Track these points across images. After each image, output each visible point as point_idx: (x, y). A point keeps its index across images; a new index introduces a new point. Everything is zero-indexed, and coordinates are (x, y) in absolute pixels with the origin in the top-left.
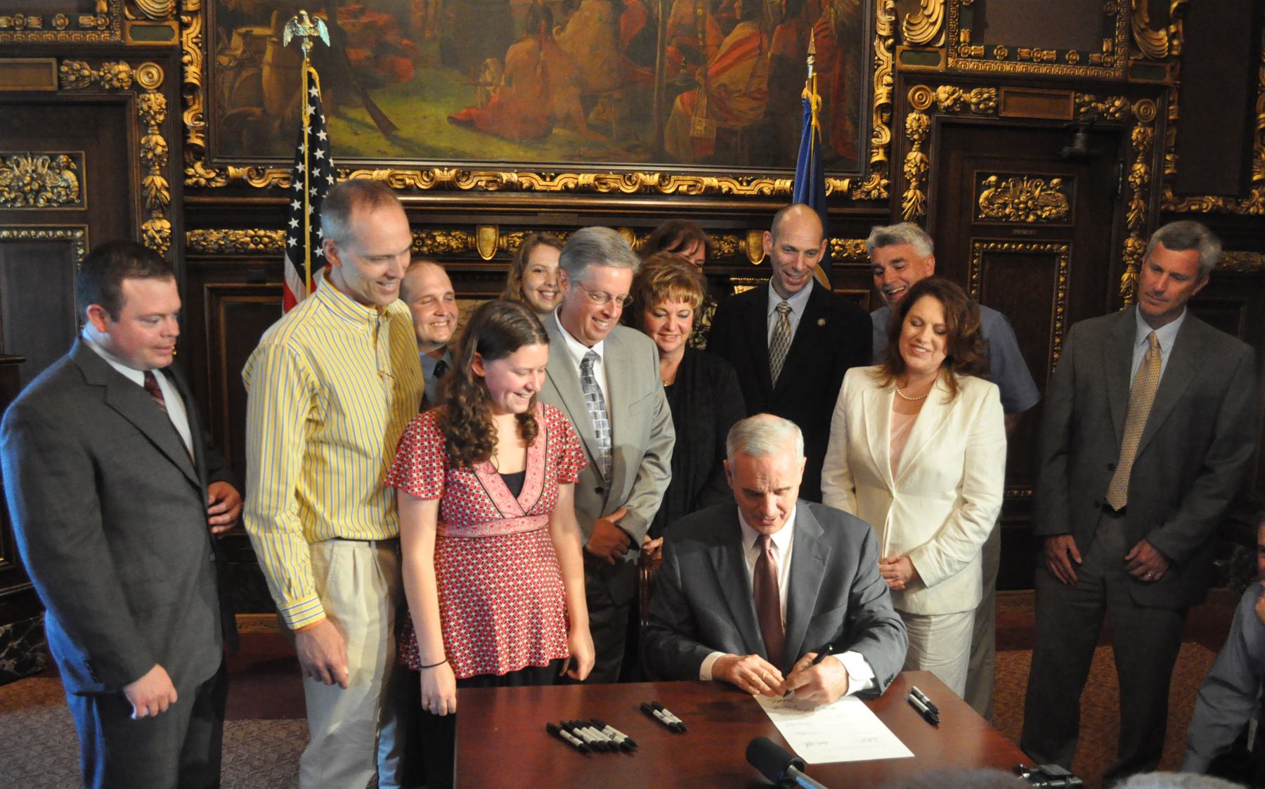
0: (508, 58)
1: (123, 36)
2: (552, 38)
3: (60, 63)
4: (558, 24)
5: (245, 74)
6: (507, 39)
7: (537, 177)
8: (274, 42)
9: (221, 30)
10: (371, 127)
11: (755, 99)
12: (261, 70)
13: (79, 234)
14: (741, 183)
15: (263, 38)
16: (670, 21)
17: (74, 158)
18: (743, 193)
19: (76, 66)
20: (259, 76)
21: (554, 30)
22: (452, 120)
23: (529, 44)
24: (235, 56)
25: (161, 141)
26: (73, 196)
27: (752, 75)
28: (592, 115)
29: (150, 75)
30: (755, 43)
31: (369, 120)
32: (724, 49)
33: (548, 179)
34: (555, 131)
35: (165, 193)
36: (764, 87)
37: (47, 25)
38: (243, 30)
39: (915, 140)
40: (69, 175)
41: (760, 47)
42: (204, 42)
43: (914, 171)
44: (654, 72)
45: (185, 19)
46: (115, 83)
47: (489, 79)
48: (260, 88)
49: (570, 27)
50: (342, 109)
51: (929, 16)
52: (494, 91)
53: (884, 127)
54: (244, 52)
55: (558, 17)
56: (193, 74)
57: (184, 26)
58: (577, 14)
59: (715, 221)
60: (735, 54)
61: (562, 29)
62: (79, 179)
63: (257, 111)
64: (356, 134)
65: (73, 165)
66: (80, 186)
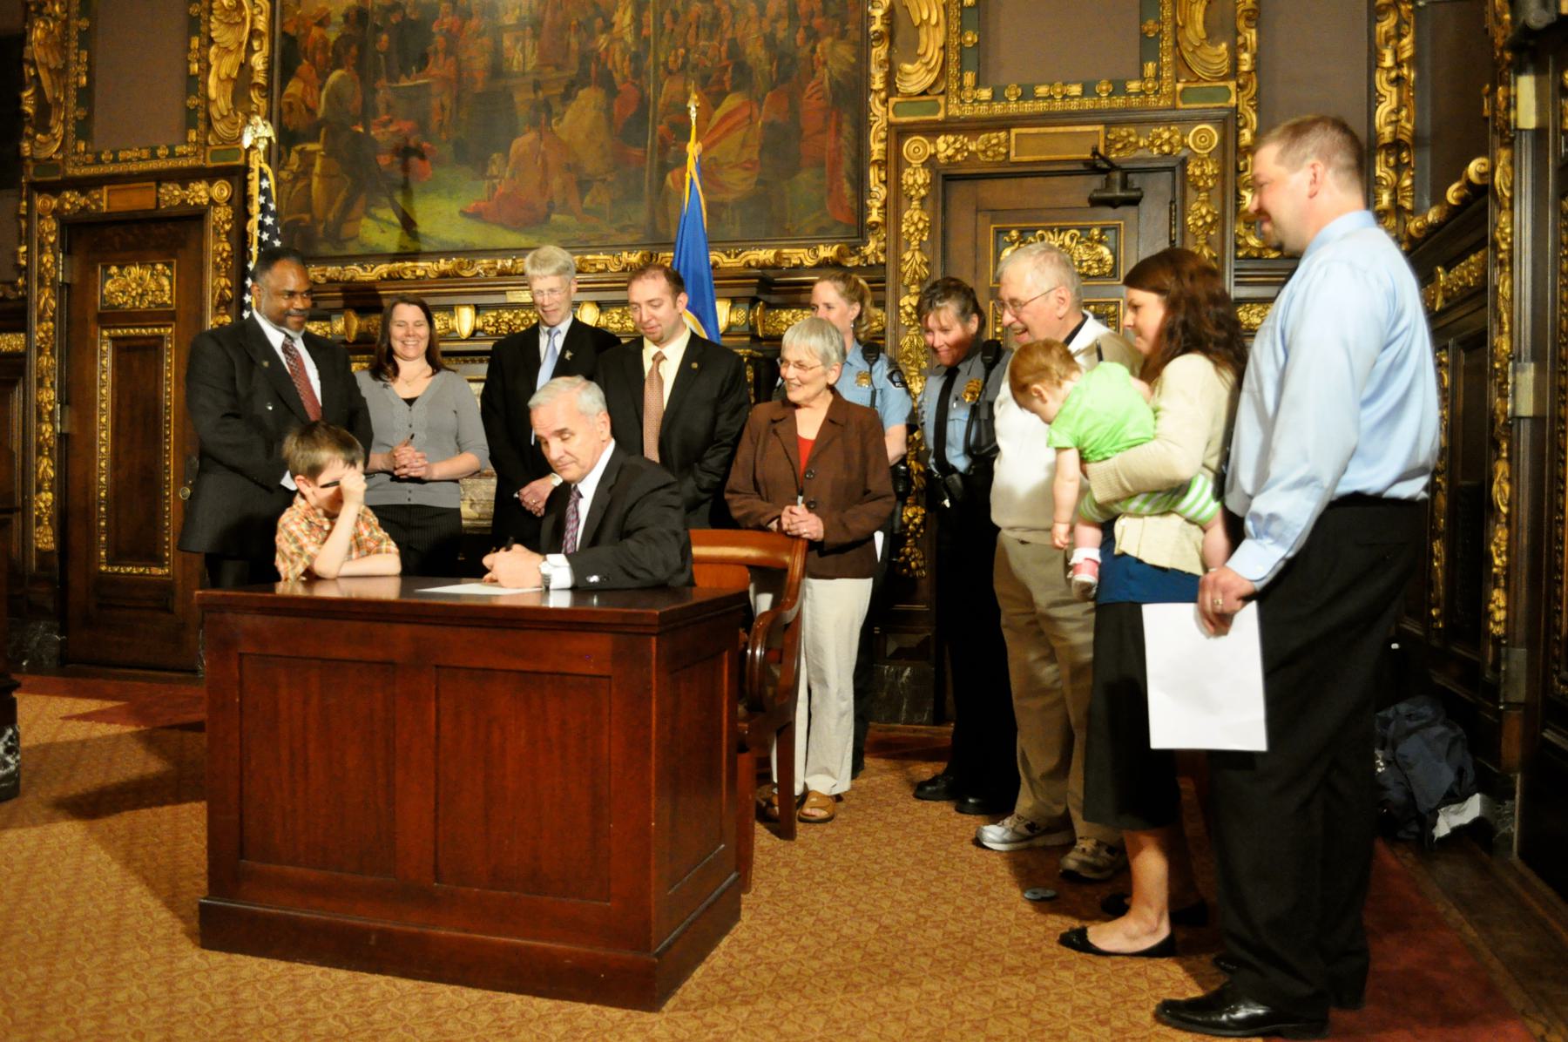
0: (512, 151)
2: (552, 131)
3: (159, 185)
4: (557, 114)
5: (300, 185)
6: (514, 134)
9: (283, 149)
10: (393, 224)
11: (747, 169)
12: (311, 180)
13: (170, 330)
14: (729, 256)
15: (314, 153)
16: (661, 100)
17: (169, 265)
19: (170, 188)
20: (309, 186)
22: (463, 213)
23: (530, 136)
24: (292, 172)
25: (228, 247)
26: (166, 298)
27: (744, 145)
28: (588, 199)
29: (221, 190)
30: (747, 112)
32: (714, 121)
34: (554, 217)
35: (228, 292)
36: (755, 156)
37: (154, 156)
38: (298, 147)
40: (165, 282)
41: (750, 117)
43: (912, 230)
44: (646, 152)
46: (198, 200)
47: (495, 173)
48: (310, 197)
49: (567, 117)
50: (373, 210)
51: (928, 63)
55: (557, 108)
58: (574, 104)
60: (725, 127)
61: (561, 120)
62: (171, 285)
63: (307, 217)
64: (383, 232)
65: (168, 272)
66: (171, 290)
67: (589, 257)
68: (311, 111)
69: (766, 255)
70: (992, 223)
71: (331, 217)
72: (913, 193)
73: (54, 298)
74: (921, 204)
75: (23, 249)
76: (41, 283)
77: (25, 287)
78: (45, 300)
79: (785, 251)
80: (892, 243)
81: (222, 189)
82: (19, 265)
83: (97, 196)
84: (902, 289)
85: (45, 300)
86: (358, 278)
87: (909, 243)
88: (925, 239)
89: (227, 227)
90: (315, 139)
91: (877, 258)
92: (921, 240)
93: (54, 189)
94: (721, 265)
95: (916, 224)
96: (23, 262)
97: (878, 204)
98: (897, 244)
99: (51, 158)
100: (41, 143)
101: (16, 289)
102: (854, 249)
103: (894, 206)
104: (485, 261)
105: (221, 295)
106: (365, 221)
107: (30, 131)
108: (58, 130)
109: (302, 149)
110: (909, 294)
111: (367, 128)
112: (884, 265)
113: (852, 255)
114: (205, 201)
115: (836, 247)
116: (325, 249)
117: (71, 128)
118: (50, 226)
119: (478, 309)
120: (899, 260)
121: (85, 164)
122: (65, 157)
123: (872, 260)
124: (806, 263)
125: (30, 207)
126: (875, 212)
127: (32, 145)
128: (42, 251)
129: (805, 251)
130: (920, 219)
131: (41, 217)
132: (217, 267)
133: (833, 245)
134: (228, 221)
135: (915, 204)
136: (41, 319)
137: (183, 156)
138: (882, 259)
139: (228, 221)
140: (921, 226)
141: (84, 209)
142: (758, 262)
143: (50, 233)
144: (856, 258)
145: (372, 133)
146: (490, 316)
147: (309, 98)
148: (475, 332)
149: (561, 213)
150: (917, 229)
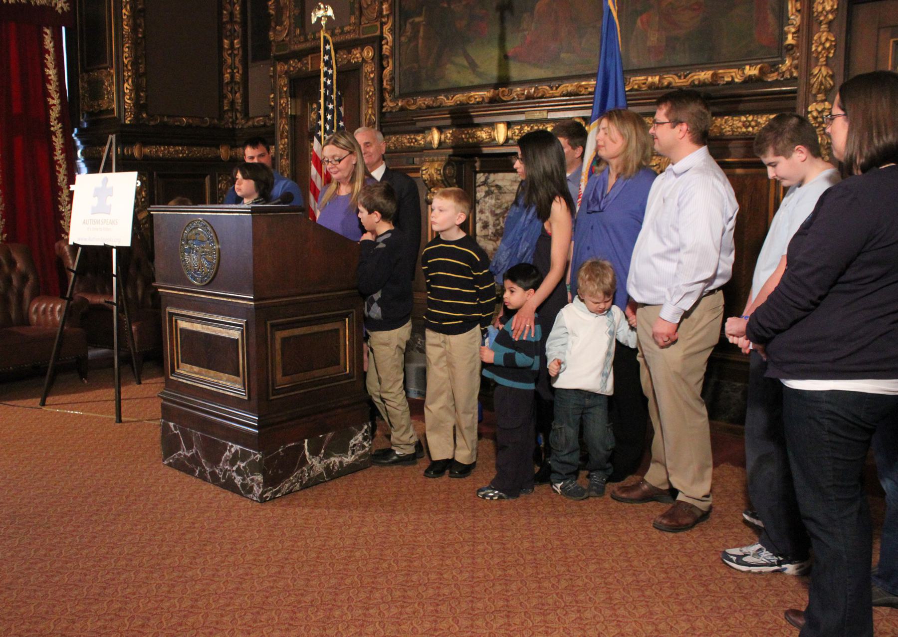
1: (359, 34)
5: (412, 45)
7: (547, 88)
10: (464, 67)
11: (695, 10)
12: (418, 42)
14: (680, 77)
15: (419, 23)
18: (679, 84)
20: (417, 45)
29: (368, 53)
31: (466, 63)
33: (554, 88)
34: (563, 55)
35: (373, 117)
38: (411, 20)
39: (821, 22)
42: (392, 31)
43: (820, 49)
45: (384, 20)
53: (797, 14)
56: (386, 49)
57: (382, 24)
59: (648, 107)
63: (416, 65)
64: (459, 72)
67: (583, 83)
69: (705, 75)
70: (892, 38)
72: (822, 18)
73: (287, 125)
74: (829, 27)
75: (272, 96)
76: (281, 117)
77: (274, 118)
78: (283, 125)
79: (721, 71)
80: (804, 61)
81: (368, 52)
82: (271, 105)
83: (305, 62)
84: (811, 98)
85: (283, 125)
86: (444, 105)
87: (817, 59)
88: (831, 55)
89: (372, 76)
91: (791, 73)
92: (827, 57)
93: (285, 59)
94: (674, 84)
95: (823, 44)
96: (272, 104)
97: (793, 30)
98: (809, 60)
99: (283, 40)
100: (280, 32)
101: (270, 119)
102: (774, 67)
103: (808, 29)
104: (518, 89)
105: (369, 119)
106: (449, 66)
107: (273, 24)
108: (286, 23)
110: (816, 101)
111: (449, 4)
112: (796, 78)
113: (772, 72)
114: (360, 60)
115: (759, 66)
116: (426, 86)
117: (293, 21)
118: (284, 81)
119: (509, 125)
120: (809, 74)
121: (300, 43)
122: (290, 39)
123: (788, 76)
124: (736, 80)
125: (275, 71)
126: (790, 37)
127: (274, 33)
128: (281, 98)
129: (736, 70)
130: (827, 40)
131: (280, 77)
132: (368, 102)
133: (757, 64)
134: (372, 72)
135: (823, 26)
136: (282, 138)
137: (349, 32)
138: (795, 74)
139: (372, 72)
140: (827, 45)
141: (300, 69)
142: (699, 81)
143: (285, 85)
144: (776, 74)
145: (452, 7)
146: (516, 129)
148: (507, 139)
150: (824, 48)
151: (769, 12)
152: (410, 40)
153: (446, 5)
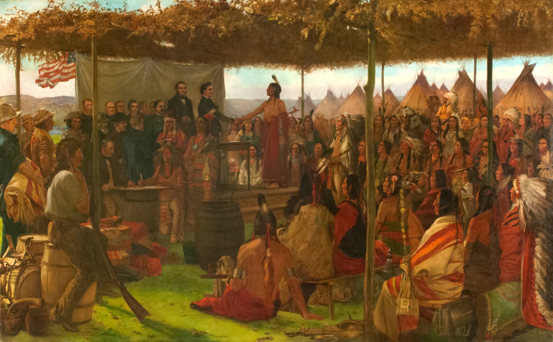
2: (277, 239)
4: (281, 226)
5: (27, 272)
8: (50, 247)
12: (40, 268)
15: (42, 243)
20: (39, 273)
21: (278, 231)
22: (195, 306)
24: (19, 259)
27: (450, 261)
32: (425, 239)
38: (25, 237)
47: (224, 273)
52: (228, 282)
54: (26, 254)
55: (281, 220)
58: (296, 218)
63: (37, 301)
64: (116, 318)
68: (38, 206)
71: (61, 301)
90: (43, 231)
106: (96, 307)
109: (29, 239)
111: (94, 225)
147: (34, 193)
149: (287, 310)
151: (537, 292)
152: (24, 265)
153: (90, 227)
